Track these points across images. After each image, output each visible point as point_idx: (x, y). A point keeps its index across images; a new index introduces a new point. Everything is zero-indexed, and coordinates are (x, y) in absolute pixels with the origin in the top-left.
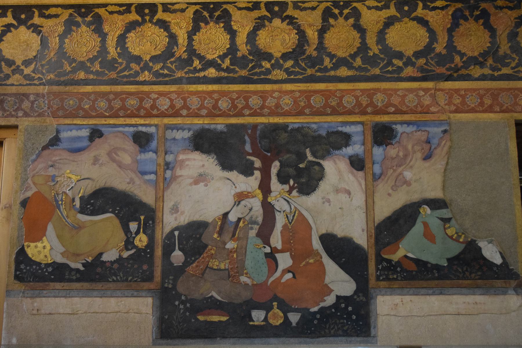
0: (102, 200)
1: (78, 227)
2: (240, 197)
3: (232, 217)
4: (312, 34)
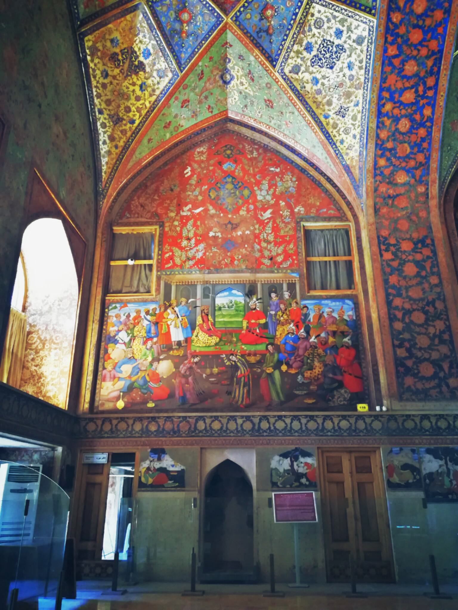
0: (405, 467)
1: (401, 474)
2: (440, 466)
3: (440, 471)
4: (451, 422)
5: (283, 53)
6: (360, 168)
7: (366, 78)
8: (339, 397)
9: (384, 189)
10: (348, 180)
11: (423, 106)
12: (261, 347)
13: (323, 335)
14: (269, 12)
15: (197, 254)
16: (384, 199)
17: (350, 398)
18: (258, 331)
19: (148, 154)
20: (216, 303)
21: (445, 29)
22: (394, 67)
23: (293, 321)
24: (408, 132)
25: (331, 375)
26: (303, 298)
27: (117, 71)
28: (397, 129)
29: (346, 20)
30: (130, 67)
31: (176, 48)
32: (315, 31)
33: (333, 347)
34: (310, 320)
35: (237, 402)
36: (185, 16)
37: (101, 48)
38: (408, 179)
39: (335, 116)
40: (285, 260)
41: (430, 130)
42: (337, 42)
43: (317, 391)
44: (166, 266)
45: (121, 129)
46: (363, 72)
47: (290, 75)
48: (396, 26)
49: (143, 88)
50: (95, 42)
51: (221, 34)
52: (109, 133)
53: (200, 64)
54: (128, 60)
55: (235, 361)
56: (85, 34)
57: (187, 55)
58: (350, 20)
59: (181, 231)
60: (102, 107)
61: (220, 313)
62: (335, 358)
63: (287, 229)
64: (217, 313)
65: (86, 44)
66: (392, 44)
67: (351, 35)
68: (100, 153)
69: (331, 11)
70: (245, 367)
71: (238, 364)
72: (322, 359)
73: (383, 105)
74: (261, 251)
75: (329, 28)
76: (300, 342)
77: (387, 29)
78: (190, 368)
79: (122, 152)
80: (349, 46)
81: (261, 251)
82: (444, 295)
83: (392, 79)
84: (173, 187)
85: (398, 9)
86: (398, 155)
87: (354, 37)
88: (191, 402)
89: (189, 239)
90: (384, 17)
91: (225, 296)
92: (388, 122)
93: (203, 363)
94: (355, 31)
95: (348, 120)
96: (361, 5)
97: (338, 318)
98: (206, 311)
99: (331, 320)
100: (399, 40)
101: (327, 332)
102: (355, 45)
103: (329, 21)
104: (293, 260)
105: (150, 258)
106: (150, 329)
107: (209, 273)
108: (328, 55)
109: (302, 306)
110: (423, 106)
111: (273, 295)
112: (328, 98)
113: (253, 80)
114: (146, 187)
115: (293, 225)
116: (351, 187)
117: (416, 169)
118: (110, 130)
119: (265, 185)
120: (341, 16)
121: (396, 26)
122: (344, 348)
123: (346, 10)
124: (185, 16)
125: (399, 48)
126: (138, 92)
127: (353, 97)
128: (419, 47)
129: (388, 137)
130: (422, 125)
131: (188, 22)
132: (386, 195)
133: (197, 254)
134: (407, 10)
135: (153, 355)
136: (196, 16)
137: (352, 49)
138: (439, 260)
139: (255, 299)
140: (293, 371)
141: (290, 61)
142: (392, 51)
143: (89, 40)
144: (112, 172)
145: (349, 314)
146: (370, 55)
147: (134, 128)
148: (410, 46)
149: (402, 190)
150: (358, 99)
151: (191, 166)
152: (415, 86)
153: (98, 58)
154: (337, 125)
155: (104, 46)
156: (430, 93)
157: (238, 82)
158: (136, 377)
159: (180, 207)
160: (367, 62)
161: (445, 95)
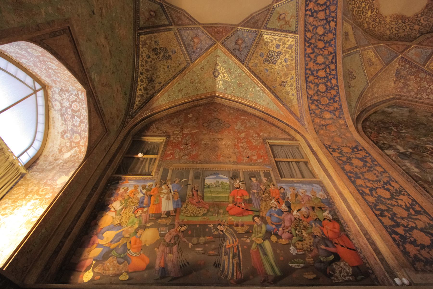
5: (248, 58)
6: (300, 110)
7: (296, 64)
8: (340, 272)
9: (318, 121)
10: (293, 118)
11: (331, 79)
12: (248, 219)
13: (303, 209)
14: (240, 42)
15: (192, 152)
16: (320, 126)
17: (352, 272)
18: (243, 205)
19: (166, 104)
20: (205, 182)
21: (335, 42)
22: (311, 59)
23: (274, 198)
24: (325, 92)
25: (323, 247)
26: (279, 182)
27: (155, 57)
28: (318, 90)
29: (282, 39)
30: (164, 56)
31: (190, 52)
32: (265, 47)
33: (316, 220)
34: (288, 198)
35: (227, 277)
36: (196, 40)
37: (148, 43)
38: (331, 116)
39: (279, 86)
40: (259, 158)
41: (337, 91)
42: (277, 51)
43: (314, 263)
44: (167, 158)
45: (152, 85)
46: (294, 61)
47: (252, 68)
48: (310, 39)
49: (169, 67)
50: (146, 40)
51: (215, 50)
52: (144, 86)
53: (202, 62)
54: (163, 53)
55: (222, 231)
56: (141, 34)
57: (196, 57)
58: (283, 38)
59: (182, 140)
60: (143, 72)
61: (208, 189)
62: (322, 231)
63: (257, 143)
64: (206, 190)
65: (140, 39)
66: (309, 47)
67: (285, 45)
68: (136, 94)
69: (273, 36)
70: (234, 237)
71: (226, 234)
72: (310, 231)
73: (308, 77)
74: (240, 152)
75: (272, 45)
76: (284, 215)
77: (305, 40)
78: (177, 236)
79: (150, 97)
80: (284, 51)
81: (240, 152)
82: (393, 178)
83: (311, 65)
84: (179, 121)
85: (310, 31)
86: (322, 103)
87: (286, 46)
88: (172, 275)
89: (187, 144)
90: (303, 34)
91: (212, 178)
92: (312, 86)
93: (190, 232)
94: (288, 43)
95: (288, 88)
96: (289, 31)
97: (312, 197)
98: (195, 188)
99: (306, 199)
100: (312, 46)
101: (307, 207)
102: (288, 50)
103: (272, 41)
104: (265, 159)
105: (157, 154)
106: (144, 200)
107: (200, 163)
108: (272, 58)
109: (279, 187)
110: (331, 79)
111: (253, 179)
112: (274, 78)
113: (231, 73)
114: (162, 120)
115: (261, 141)
116: (296, 121)
117: (335, 111)
118: (146, 85)
119: (239, 123)
120: (279, 38)
121: (310, 39)
122: (326, 221)
123: (281, 34)
124: (196, 40)
125: (313, 49)
126: (166, 69)
127: (289, 75)
128: (323, 50)
129: (314, 94)
130: (332, 88)
131: (198, 43)
132: (321, 124)
133: (192, 152)
134: (314, 32)
135: (140, 223)
136: (202, 41)
137: (286, 52)
138: (375, 158)
139: (238, 181)
140: (283, 241)
141: (251, 61)
142: (309, 50)
143: (143, 38)
144: (141, 106)
145: (320, 194)
146: (297, 52)
147: (160, 87)
148: (318, 49)
149: (330, 122)
150: (292, 75)
151: (192, 113)
152: (324, 68)
153: (146, 47)
154: (281, 91)
155: (150, 43)
156: (333, 73)
157: (222, 76)
158: (116, 244)
159: (182, 129)
160: (296, 56)
161: (342, 74)
